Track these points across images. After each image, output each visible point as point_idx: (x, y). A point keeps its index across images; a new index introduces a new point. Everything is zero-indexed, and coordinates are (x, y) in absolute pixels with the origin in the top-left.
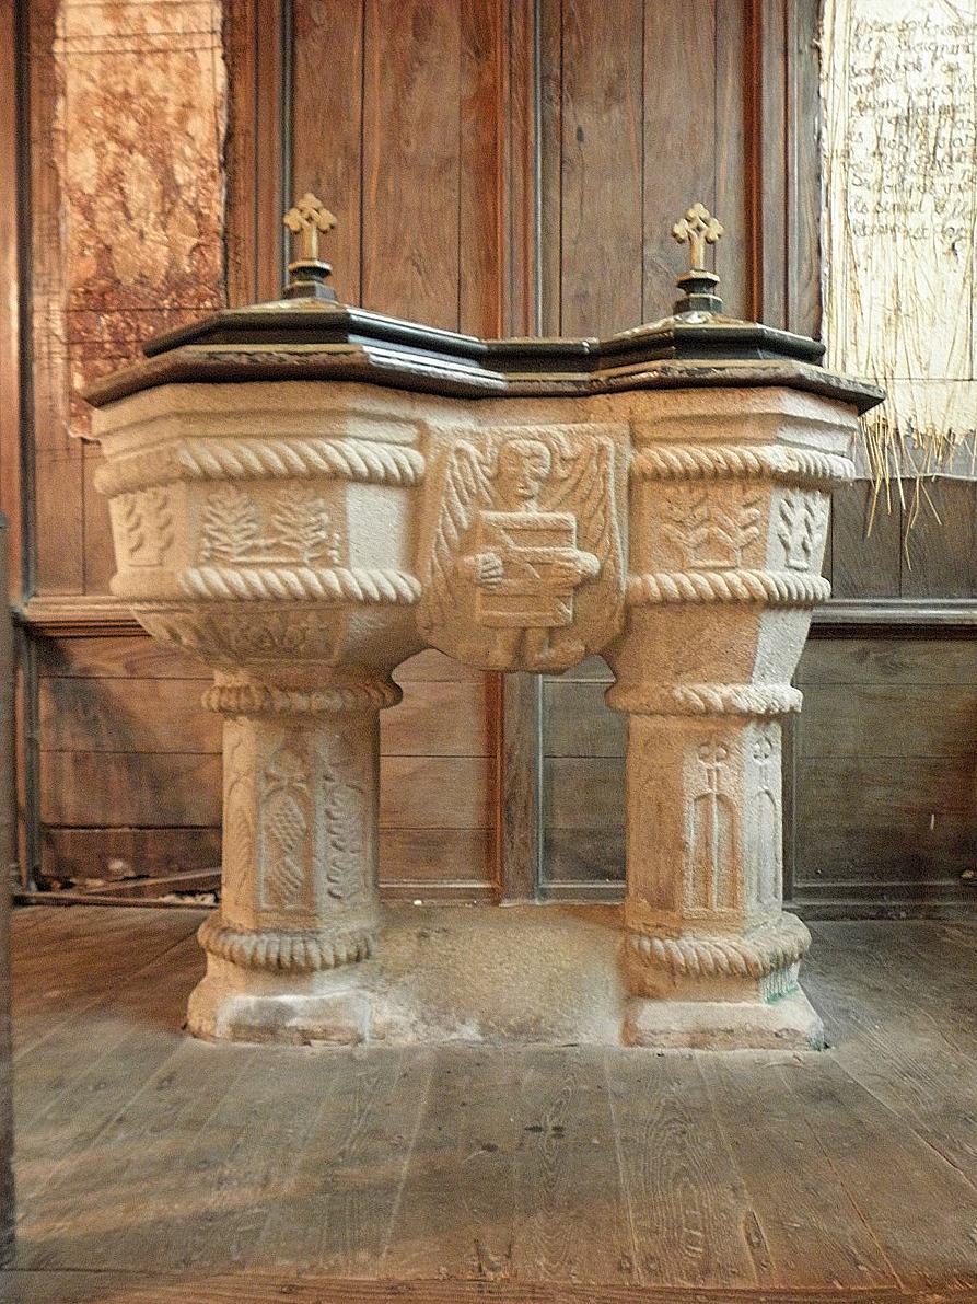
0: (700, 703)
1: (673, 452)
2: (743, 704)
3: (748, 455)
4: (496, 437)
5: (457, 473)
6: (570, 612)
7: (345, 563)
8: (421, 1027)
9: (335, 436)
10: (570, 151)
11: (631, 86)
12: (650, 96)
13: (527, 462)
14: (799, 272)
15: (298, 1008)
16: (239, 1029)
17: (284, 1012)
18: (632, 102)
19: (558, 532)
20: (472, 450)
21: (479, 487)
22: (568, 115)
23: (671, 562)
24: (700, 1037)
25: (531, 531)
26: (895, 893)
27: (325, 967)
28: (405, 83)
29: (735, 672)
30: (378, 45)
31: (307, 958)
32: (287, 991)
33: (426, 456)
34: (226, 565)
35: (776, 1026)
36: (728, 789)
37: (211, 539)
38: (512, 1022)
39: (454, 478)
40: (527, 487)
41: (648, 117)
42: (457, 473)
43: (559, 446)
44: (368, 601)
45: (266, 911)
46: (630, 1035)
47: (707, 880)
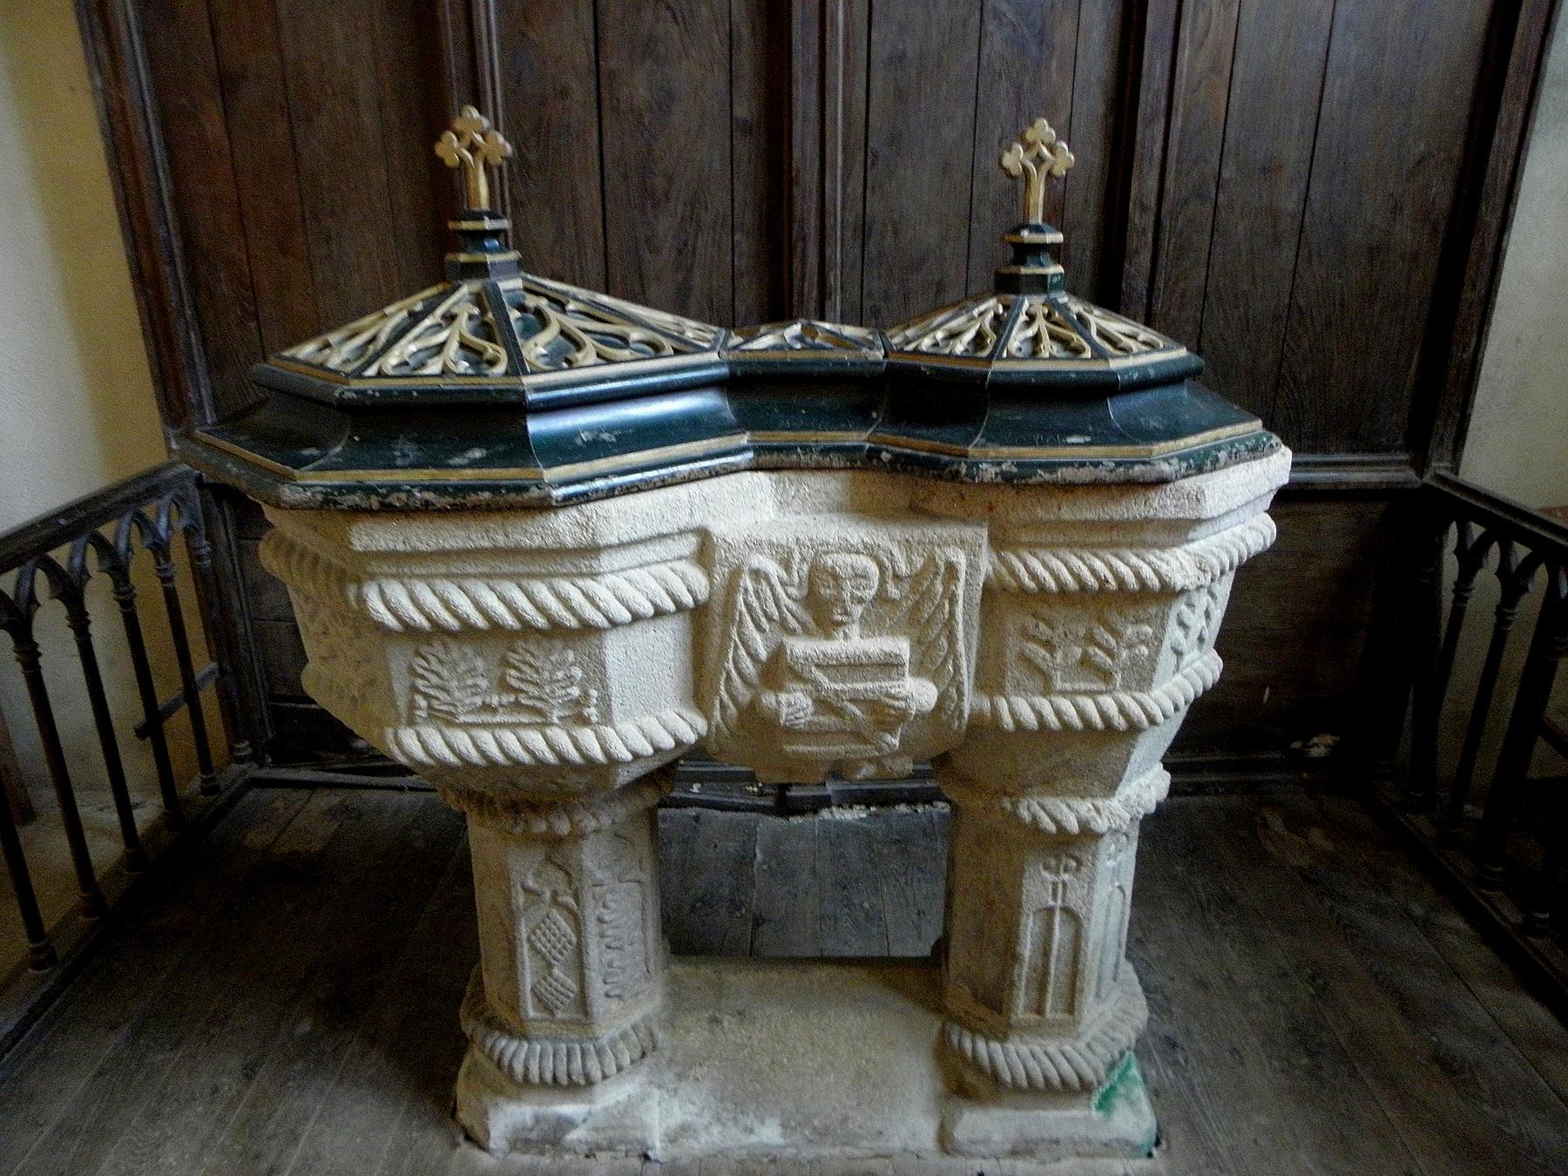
0: (1052, 827)
1: (1045, 564)
3: (1147, 572)
4: (805, 551)
5: (753, 599)
6: (896, 742)
7: (607, 717)
8: (715, 1130)
9: (582, 575)
13: (848, 585)
14: (1194, 28)
15: (579, 1119)
16: (520, 1142)
17: (567, 1124)
19: (888, 665)
20: (772, 568)
21: (780, 612)
23: (1030, 685)
25: (854, 666)
27: (605, 1077)
29: (1097, 787)
31: (587, 1076)
32: (561, 1103)
33: (710, 576)
34: (450, 724)
35: (1106, 1136)
36: (1074, 901)
37: (426, 696)
38: (816, 1123)
39: (748, 605)
40: (846, 613)
42: (753, 599)
43: (892, 561)
45: (534, 1020)
46: (945, 1142)
47: (1042, 988)
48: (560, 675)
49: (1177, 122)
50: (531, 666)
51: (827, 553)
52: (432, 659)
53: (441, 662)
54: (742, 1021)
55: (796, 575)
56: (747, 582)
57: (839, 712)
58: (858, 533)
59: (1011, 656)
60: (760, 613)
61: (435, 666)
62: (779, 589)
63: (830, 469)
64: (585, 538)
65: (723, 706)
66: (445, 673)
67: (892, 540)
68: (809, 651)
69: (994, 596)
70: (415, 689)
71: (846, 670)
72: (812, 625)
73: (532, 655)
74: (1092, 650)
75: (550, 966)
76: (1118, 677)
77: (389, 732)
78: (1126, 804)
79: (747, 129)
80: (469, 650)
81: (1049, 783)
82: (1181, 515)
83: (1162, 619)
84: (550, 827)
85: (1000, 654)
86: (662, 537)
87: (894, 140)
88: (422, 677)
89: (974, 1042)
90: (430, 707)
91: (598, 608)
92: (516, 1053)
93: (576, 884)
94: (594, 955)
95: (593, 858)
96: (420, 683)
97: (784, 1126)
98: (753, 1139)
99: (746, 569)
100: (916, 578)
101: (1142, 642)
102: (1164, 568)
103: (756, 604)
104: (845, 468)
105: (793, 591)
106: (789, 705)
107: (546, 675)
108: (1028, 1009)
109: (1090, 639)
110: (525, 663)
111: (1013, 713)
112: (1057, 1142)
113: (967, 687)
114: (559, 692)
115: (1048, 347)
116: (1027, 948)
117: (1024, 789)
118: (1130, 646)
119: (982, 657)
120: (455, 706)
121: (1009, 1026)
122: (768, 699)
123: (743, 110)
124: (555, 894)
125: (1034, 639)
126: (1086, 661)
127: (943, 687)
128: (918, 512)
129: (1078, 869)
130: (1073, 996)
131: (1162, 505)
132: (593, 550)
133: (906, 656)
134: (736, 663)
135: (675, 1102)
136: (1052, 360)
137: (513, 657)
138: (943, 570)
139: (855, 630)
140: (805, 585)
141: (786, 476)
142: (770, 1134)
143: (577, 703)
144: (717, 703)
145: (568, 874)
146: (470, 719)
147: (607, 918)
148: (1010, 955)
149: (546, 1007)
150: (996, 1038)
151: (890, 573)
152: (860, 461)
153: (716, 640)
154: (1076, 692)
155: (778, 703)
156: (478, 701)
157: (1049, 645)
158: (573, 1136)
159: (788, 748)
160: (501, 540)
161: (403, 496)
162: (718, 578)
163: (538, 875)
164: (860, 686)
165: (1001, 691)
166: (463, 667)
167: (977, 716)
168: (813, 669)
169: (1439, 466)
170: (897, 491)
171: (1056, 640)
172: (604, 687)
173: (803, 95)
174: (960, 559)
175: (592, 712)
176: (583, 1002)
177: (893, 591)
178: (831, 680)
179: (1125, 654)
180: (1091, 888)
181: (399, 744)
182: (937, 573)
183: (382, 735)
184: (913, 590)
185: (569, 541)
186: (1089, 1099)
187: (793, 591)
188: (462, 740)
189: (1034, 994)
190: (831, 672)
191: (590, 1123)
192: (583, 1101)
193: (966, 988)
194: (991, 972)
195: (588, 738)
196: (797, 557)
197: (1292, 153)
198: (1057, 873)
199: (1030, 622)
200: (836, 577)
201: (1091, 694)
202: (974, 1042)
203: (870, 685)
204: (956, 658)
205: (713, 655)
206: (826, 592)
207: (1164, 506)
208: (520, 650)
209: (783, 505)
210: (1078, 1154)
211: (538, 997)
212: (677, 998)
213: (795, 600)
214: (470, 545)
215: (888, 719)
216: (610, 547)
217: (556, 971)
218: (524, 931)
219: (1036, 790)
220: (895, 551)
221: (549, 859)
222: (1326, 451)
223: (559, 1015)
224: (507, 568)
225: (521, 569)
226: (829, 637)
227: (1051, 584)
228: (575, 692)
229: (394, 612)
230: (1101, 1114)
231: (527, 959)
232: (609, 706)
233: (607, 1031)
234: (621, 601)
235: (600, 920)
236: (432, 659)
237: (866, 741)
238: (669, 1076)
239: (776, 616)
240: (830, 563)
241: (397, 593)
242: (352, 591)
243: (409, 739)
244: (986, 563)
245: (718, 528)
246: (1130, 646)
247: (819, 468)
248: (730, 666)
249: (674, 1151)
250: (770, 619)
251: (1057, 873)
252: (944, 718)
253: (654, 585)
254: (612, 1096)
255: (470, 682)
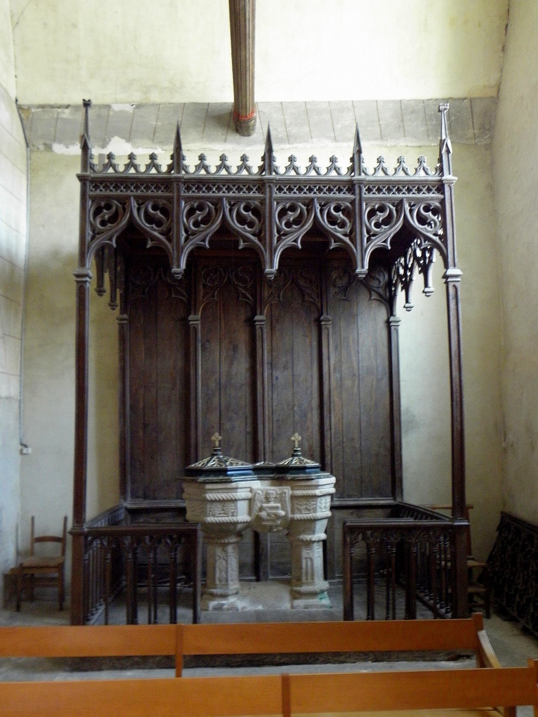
2: (313, 539)
10: (274, 382)
11: (290, 365)
12: (295, 369)
16: (215, 609)
17: (223, 605)
18: (290, 370)
19: (277, 508)
22: (274, 373)
24: (306, 607)
28: (231, 364)
30: (224, 354)
36: (311, 555)
41: (295, 374)
44: (241, 523)
46: (292, 607)
49: (333, 431)
56: (257, 495)
58: (273, 488)
69: (293, 497)
79: (250, 433)
81: (304, 532)
87: (278, 435)
94: (229, 569)
95: (230, 549)
115: (298, 463)
116: (304, 566)
117: (300, 534)
122: (260, 514)
123: (249, 430)
125: (298, 504)
128: (280, 485)
131: (313, 483)
132: (237, 488)
136: (298, 464)
141: (263, 481)
142: (260, 608)
143: (233, 513)
148: (301, 568)
152: (273, 479)
158: (225, 607)
169: (399, 500)
173: (260, 427)
176: (227, 580)
197: (356, 436)
212: (242, 585)
222: (375, 497)
241: (210, 495)
244: (291, 492)
254: (232, 600)
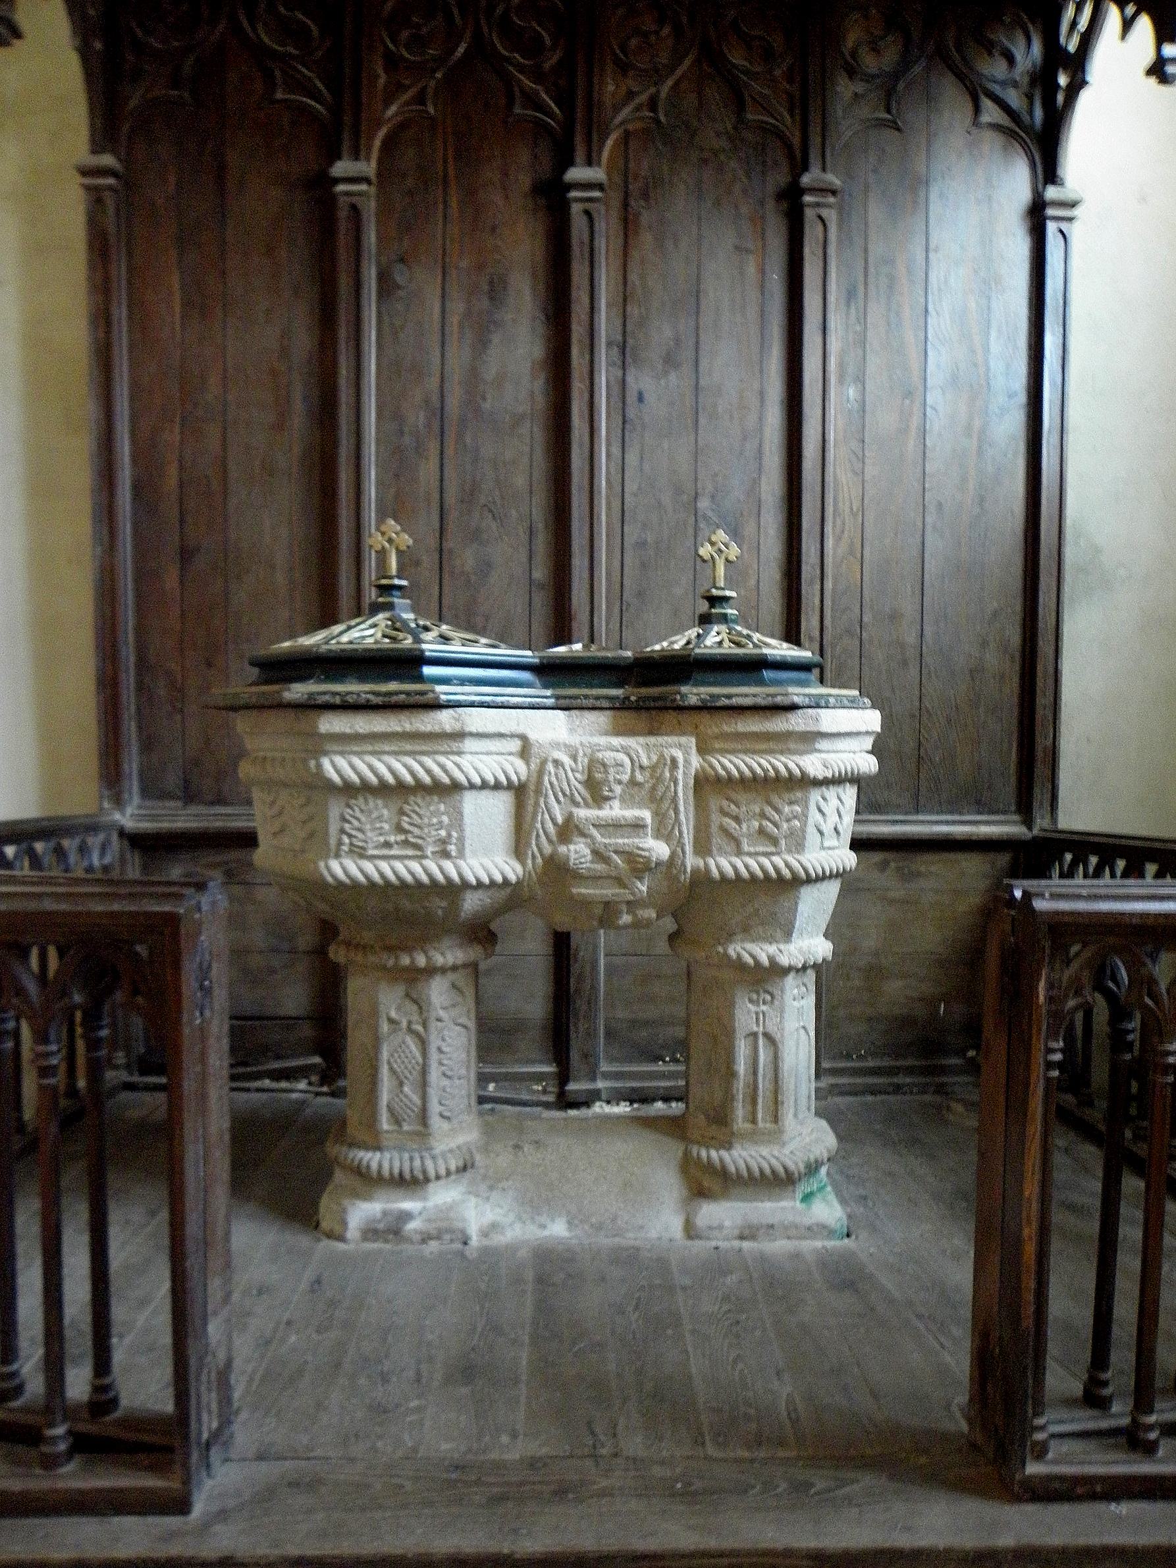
0: (750, 961)
1: (731, 761)
2: (784, 961)
3: (792, 765)
4: (585, 749)
5: (554, 779)
6: (644, 889)
7: (461, 854)
8: (518, 1227)
9: (453, 753)
10: (631, 413)
11: (687, 354)
12: (704, 364)
13: (611, 770)
14: (834, 526)
15: (416, 1212)
16: (371, 1232)
17: (406, 1216)
18: (687, 368)
19: (637, 826)
20: (567, 760)
21: (571, 790)
22: (630, 379)
23: (728, 849)
24: (748, 1233)
25: (616, 826)
26: (910, 1071)
27: (438, 1178)
28: (482, 344)
29: (779, 934)
30: (457, 307)
31: (424, 1172)
32: (404, 1199)
33: (528, 764)
34: (362, 856)
35: (807, 1221)
36: (772, 1028)
37: (350, 836)
38: (594, 1220)
39: (551, 784)
40: (611, 790)
41: (702, 382)
42: (554, 779)
43: (638, 757)
44: (480, 885)
45: (387, 1132)
46: (690, 1231)
47: (754, 1102)
48: (435, 820)
49: (829, 585)
50: (417, 814)
51: (599, 751)
52: (356, 809)
53: (362, 811)
54: (538, 1148)
55: (580, 764)
56: (550, 767)
57: (605, 860)
58: (616, 741)
59: (714, 829)
60: (558, 789)
61: (358, 814)
62: (570, 774)
63: (601, 709)
64: (457, 727)
65: (534, 857)
66: (363, 819)
67: (638, 743)
68: (589, 815)
69: (704, 784)
70: (342, 831)
71: (611, 829)
72: (590, 800)
73: (419, 806)
74: (766, 823)
75: (401, 1084)
76: (783, 842)
77: (322, 864)
78: (800, 951)
79: (542, 587)
80: (380, 802)
81: (746, 931)
82: (808, 729)
83: (806, 802)
84: (413, 961)
85: (708, 826)
86: (501, 735)
87: (640, 594)
88: (349, 822)
89: (708, 1152)
90: (351, 844)
91: (463, 772)
92: (372, 1159)
93: (425, 1014)
94: (434, 1075)
95: (438, 992)
96: (347, 826)
97: (569, 1223)
98: (546, 1233)
99: (550, 759)
100: (653, 768)
101: (795, 817)
102: (801, 763)
103: (555, 783)
104: (610, 709)
105: (578, 776)
106: (576, 852)
107: (426, 820)
108: (745, 1120)
109: (763, 815)
110: (414, 811)
111: (718, 866)
112: (772, 1226)
113: (689, 849)
114: (434, 833)
115: (726, 644)
116: (741, 1067)
117: (730, 937)
118: (788, 821)
119: (697, 829)
120: (366, 842)
121: (733, 1133)
122: (562, 849)
123: (539, 574)
124: (410, 1023)
125: (726, 814)
126: (762, 831)
127: (674, 848)
128: (651, 732)
129: (772, 1002)
130: (777, 1110)
131: (796, 722)
132: (460, 735)
133: (649, 821)
134: (542, 824)
135: (488, 1206)
136: (728, 649)
137: (407, 808)
138: (669, 762)
139: (616, 803)
140: (586, 772)
141: (573, 712)
142: (558, 1229)
143: (444, 842)
144: (530, 853)
145: (420, 1008)
146: (376, 852)
147: (444, 1049)
148: (732, 1074)
149: (397, 1120)
150: (724, 1148)
151: (637, 764)
152: (621, 706)
153: (530, 809)
154: (757, 854)
155: (569, 850)
156: (382, 839)
157: (737, 819)
158: (412, 1226)
159: (574, 891)
160: (408, 727)
161: (355, 696)
162: (533, 766)
163: (398, 1009)
164: (620, 841)
165: (711, 855)
166: (374, 815)
167: (695, 871)
168: (591, 827)
169: (1041, 822)
170: (641, 720)
171: (742, 816)
172: (461, 830)
173: (579, 562)
174: (679, 755)
175: (452, 848)
176: (423, 1117)
177: (639, 777)
178: (602, 836)
179: (785, 826)
180: (782, 1017)
181: (328, 868)
182: (665, 764)
183: (317, 868)
184: (652, 777)
185: (448, 729)
186: (794, 1191)
187: (578, 776)
188: (369, 867)
189: (749, 1108)
190: (602, 830)
191: (424, 1216)
192: (420, 1199)
193: (702, 1116)
194: (719, 1095)
195: (448, 866)
196: (581, 753)
197: (909, 607)
198: (758, 1005)
199: (725, 803)
200: (604, 765)
201: (766, 855)
202: (708, 1152)
203: (626, 841)
204: (680, 826)
205: (528, 818)
206: (598, 776)
207: (798, 724)
208: (412, 803)
209: (572, 731)
210: (789, 1238)
211: (390, 1109)
212: (489, 1132)
213: (579, 782)
214: (389, 730)
215: (639, 866)
216: (471, 735)
217: (406, 1089)
218: (385, 1054)
219: (739, 937)
220: (640, 751)
221: (407, 995)
222: (961, 813)
223: (406, 1127)
224: (408, 747)
225: (418, 748)
226: (600, 808)
227: (735, 773)
228: (443, 833)
229: (338, 771)
230: (804, 1205)
231: (385, 1079)
232: (463, 845)
233: (440, 1145)
234: (476, 769)
235: (440, 1050)
236: (356, 809)
237: (625, 887)
238: (483, 1187)
239: (568, 793)
240: (601, 756)
241: (341, 762)
242: (312, 763)
243: (335, 865)
244: (696, 761)
245: (533, 736)
246: (788, 821)
247: (594, 708)
248: (539, 826)
249: (486, 1242)
250: (564, 795)
251: (758, 1005)
252: (675, 872)
253: (495, 765)
254: (442, 1196)
255: (378, 825)
